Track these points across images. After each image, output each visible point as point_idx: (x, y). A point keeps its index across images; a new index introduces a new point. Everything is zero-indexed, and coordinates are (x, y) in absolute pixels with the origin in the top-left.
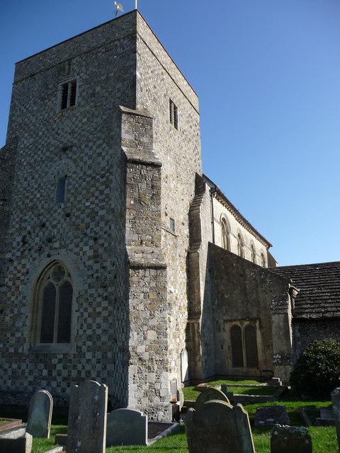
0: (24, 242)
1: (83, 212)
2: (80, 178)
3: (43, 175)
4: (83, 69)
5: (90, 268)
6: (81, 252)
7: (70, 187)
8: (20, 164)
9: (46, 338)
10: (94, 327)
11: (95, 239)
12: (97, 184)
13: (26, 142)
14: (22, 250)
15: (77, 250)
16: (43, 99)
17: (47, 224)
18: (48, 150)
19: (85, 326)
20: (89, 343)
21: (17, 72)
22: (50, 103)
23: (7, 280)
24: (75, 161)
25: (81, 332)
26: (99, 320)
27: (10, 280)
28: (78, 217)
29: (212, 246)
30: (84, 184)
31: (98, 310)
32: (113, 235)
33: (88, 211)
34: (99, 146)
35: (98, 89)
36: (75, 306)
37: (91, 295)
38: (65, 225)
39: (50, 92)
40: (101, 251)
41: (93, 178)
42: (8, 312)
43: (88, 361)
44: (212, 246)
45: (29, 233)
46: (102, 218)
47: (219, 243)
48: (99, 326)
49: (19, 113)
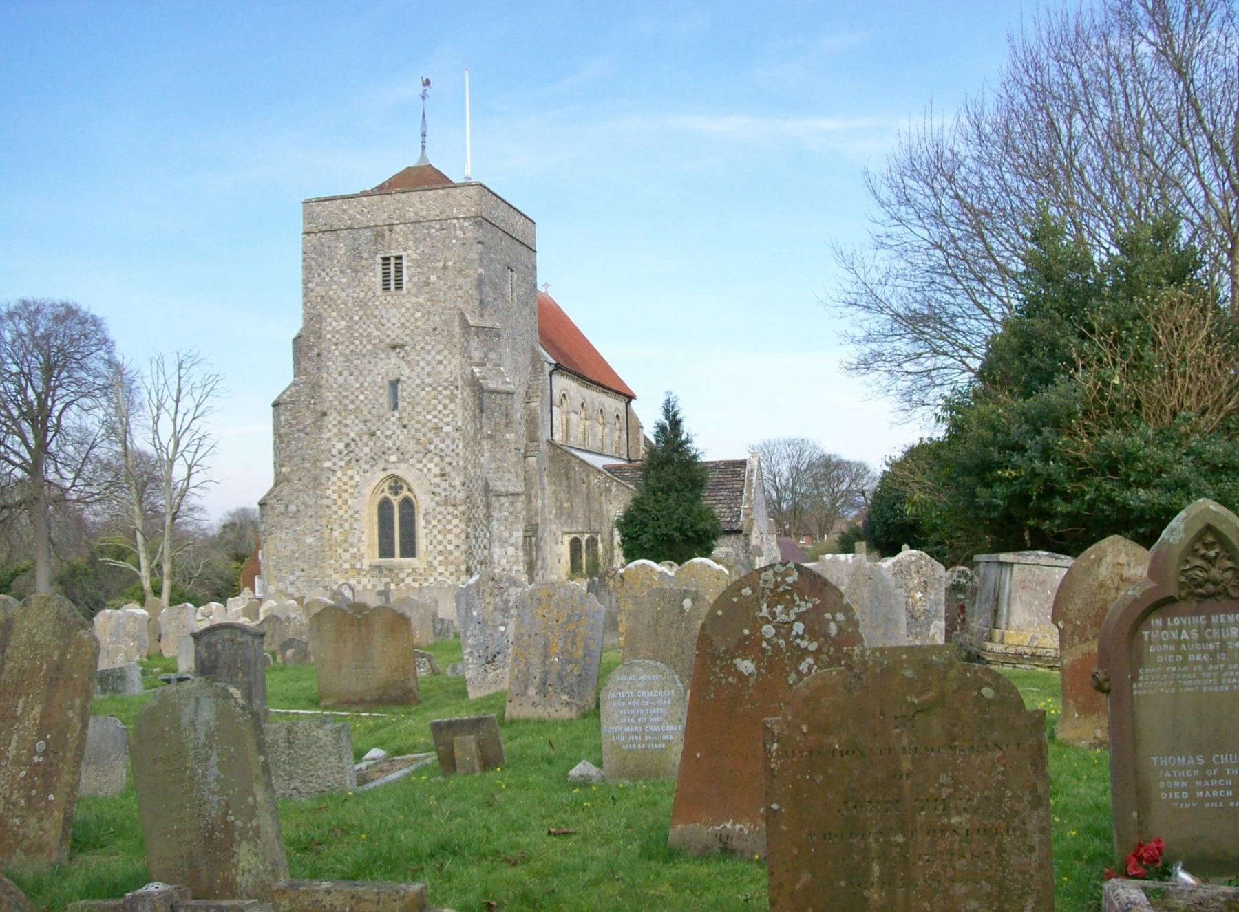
1: (424, 425)
2: (418, 386)
3: (365, 373)
4: (411, 243)
6: (425, 470)
7: (405, 394)
8: (329, 352)
9: (386, 550)
10: (445, 543)
12: (440, 397)
14: (347, 459)
15: (420, 466)
16: (355, 271)
17: (378, 433)
18: (369, 342)
19: (435, 542)
20: (441, 558)
21: (309, 217)
22: (366, 279)
23: (329, 492)
24: (408, 363)
25: (431, 548)
26: (449, 537)
27: (334, 492)
28: (417, 430)
30: (423, 393)
31: (449, 527)
32: (461, 454)
33: (430, 425)
34: (439, 352)
35: (433, 278)
37: (440, 513)
38: (402, 437)
39: (364, 263)
40: (448, 469)
41: (434, 389)
42: (336, 527)
43: (441, 574)
45: (353, 440)
46: (447, 434)
48: (450, 542)
49: (317, 280)
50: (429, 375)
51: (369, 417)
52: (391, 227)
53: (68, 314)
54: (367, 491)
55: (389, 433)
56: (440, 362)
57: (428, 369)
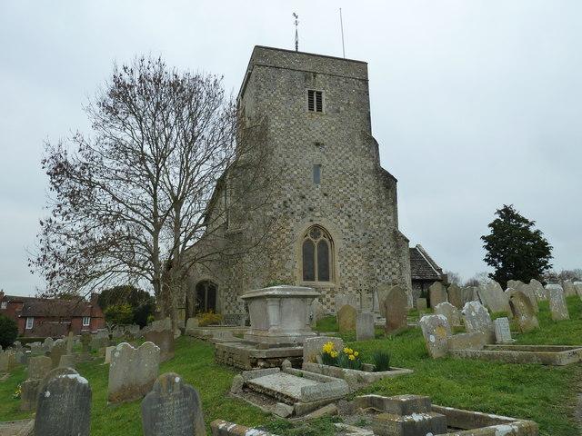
11: (349, 216)
13: (276, 123)
17: (307, 197)
24: (327, 156)
26: (355, 268)
30: (337, 176)
32: (363, 215)
34: (346, 152)
35: (342, 109)
46: (353, 203)
49: (264, 94)
50: (340, 164)
51: (300, 186)
52: (315, 74)
55: (315, 197)
56: (348, 158)
57: (339, 161)
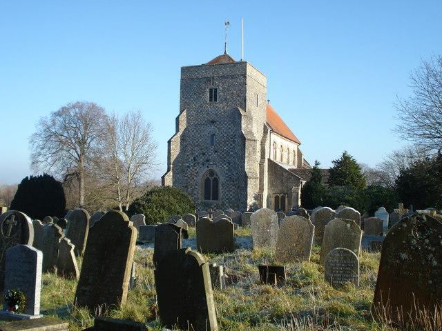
0: (195, 159)
5: (227, 174)
9: (207, 197)
11: (229, 163)
29: (269, 160)
35: (228, 97)
36: (220, 187)
44: (269, 160)
46: (232, 155)
47: (272, 159)
53: (93, 107)
54: (201, 175)
